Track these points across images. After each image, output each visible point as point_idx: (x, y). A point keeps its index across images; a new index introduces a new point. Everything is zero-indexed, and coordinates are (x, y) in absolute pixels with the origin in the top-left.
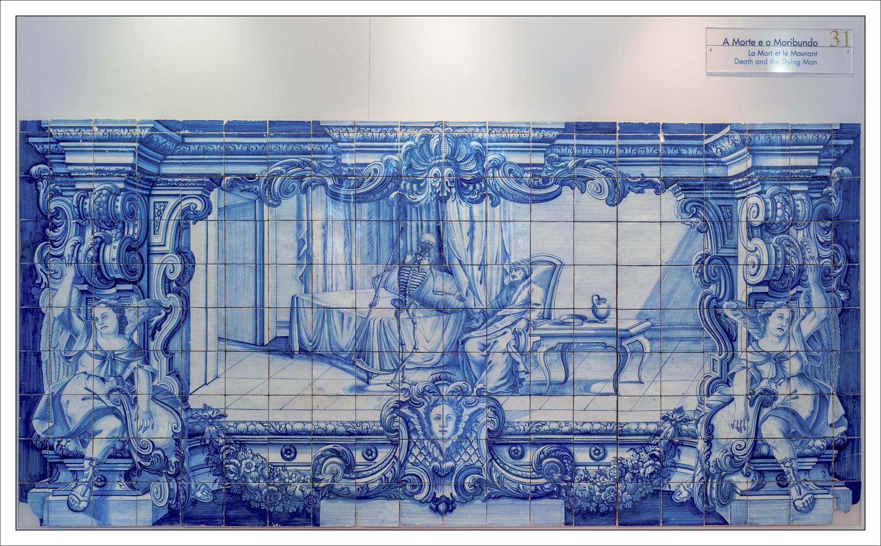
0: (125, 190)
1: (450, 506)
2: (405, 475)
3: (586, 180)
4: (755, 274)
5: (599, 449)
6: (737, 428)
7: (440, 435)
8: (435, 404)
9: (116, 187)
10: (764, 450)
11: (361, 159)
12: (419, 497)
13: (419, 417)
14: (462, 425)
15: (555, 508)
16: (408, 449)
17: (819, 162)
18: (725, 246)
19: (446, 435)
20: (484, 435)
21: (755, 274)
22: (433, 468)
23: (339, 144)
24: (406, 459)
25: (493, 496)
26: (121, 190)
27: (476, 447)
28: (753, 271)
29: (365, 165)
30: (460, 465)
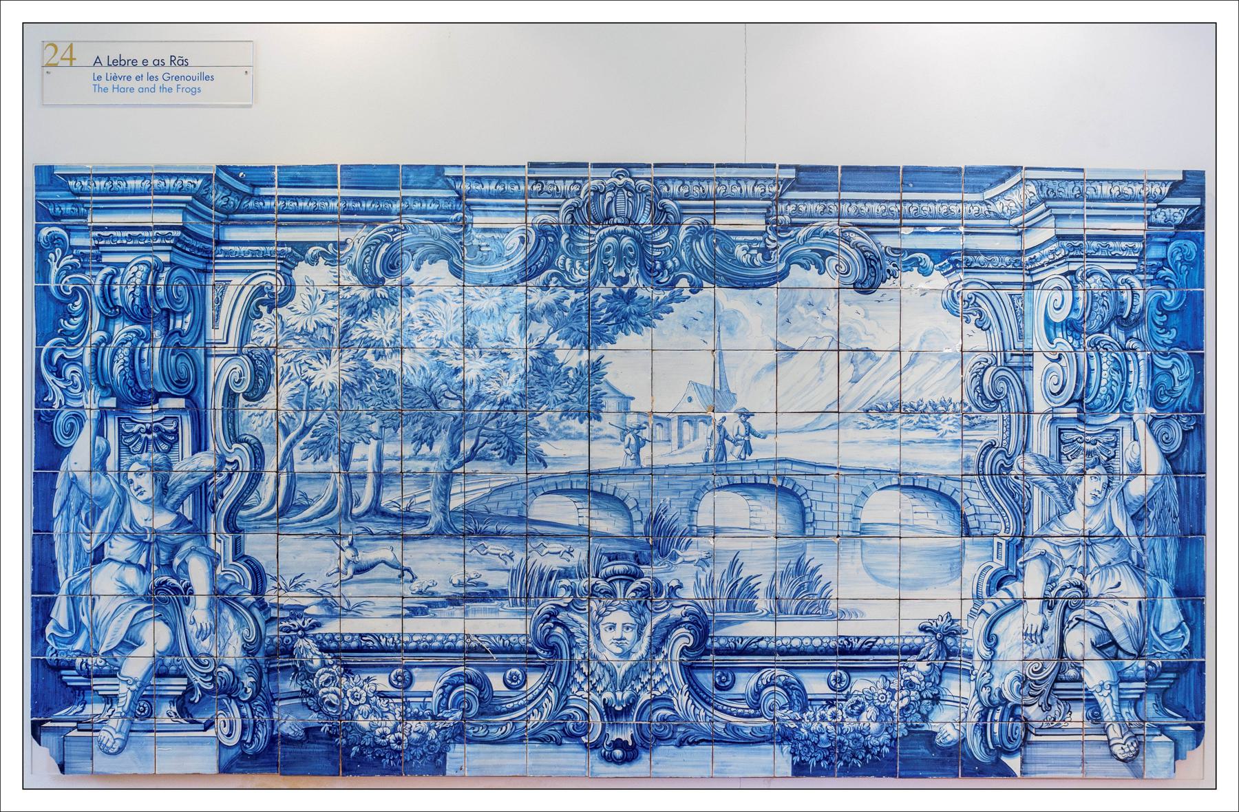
0: (171, 264)
1: (630, 753)
2: (564, 708)
3: (825, 254)
4: (1059, 393)
9: (158, 260)
12: (584, 739)
16: (569, 673)
21: (1059, 393)
25: (690, 740)
26: (165, 264)
30: (645, 697)
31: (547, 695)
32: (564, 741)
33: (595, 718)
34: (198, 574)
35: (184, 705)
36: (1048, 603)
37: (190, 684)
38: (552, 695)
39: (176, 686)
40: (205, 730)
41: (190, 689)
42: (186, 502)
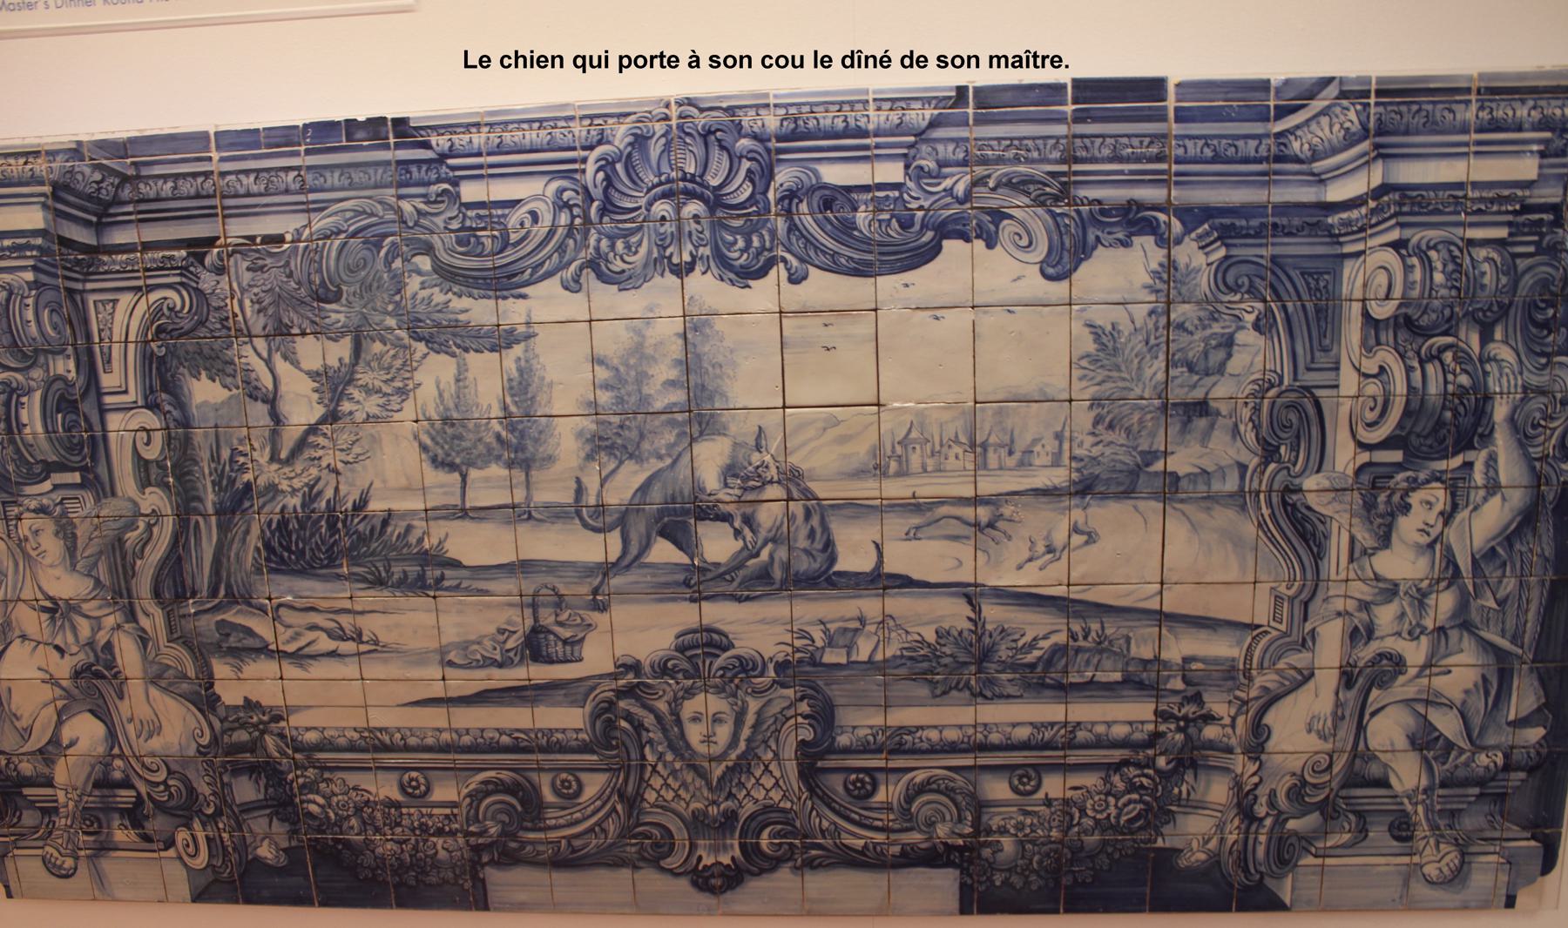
5: (1026, 777)
6: (1318, 732)
7: (702, 749)
8: (690, 693)
10: (1374, 770)
11: (502, 190)
12: (669, 862)
13: (659, 718)
14: (746, 732)
15: (945, 881)
17: (1540, 175)
18: (1313, 366)
19: (716, 750)
20: (789, 751)
22: (693, 812)
23: (451, 162)
24: (639, 795)
27: (777, 774)
28: (1370, 416)
29: (513, 204)
30: (749, 808)
31: (614, 809)
32: (641, 864)
33: (680, 834)
34: (128, 656)
35: (134, 816)
36: (1347, 677)
37: (139, 796)
38: (619, 807)
39: (125, 796)
40: (166, 849)
41: (139, 801)
42: (100, 564)
